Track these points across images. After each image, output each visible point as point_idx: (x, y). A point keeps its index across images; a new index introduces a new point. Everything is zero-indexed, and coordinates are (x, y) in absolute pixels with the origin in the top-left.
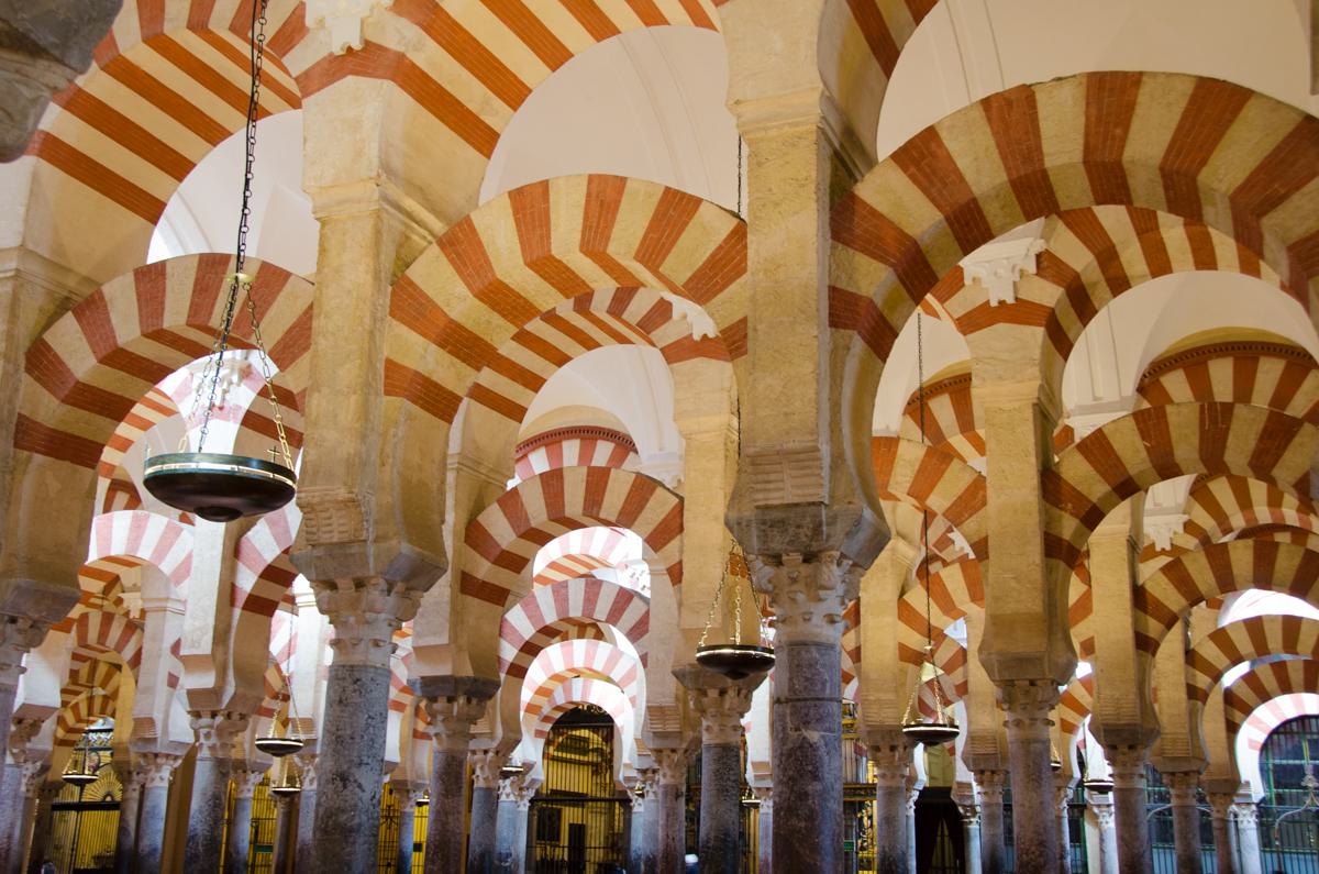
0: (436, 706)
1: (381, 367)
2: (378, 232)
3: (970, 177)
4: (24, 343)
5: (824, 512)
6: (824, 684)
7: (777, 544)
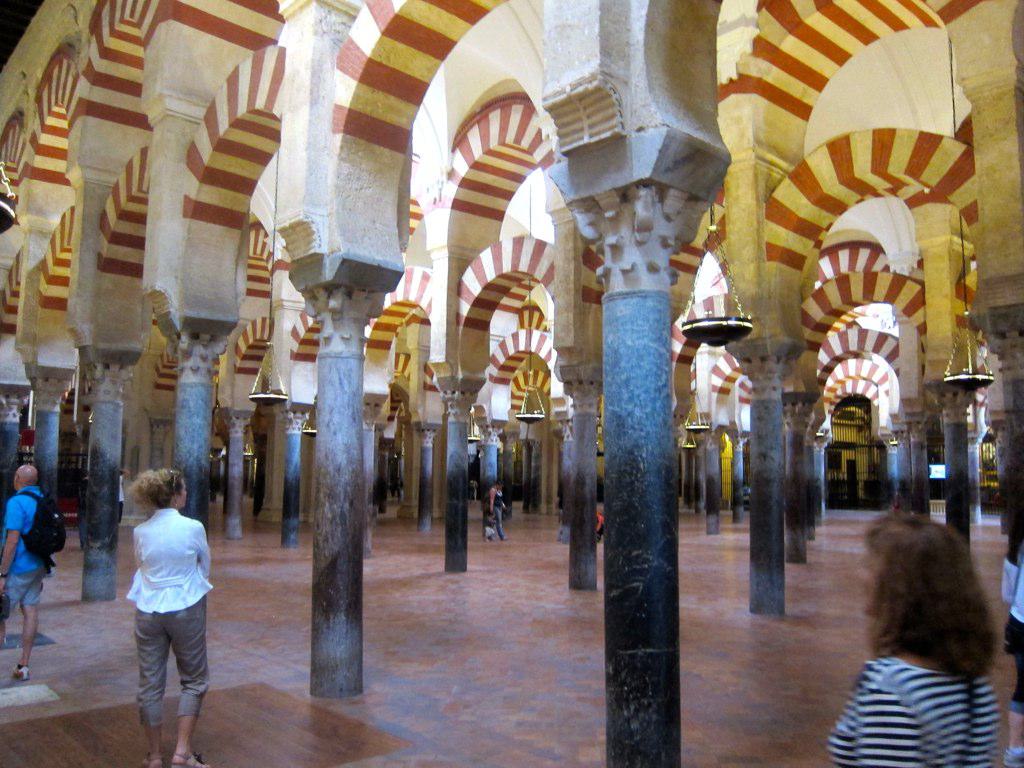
0: (786, 408)
1: (764, 247)
2: (756, 176)
4: (580, 253)
7: (1003, 327)
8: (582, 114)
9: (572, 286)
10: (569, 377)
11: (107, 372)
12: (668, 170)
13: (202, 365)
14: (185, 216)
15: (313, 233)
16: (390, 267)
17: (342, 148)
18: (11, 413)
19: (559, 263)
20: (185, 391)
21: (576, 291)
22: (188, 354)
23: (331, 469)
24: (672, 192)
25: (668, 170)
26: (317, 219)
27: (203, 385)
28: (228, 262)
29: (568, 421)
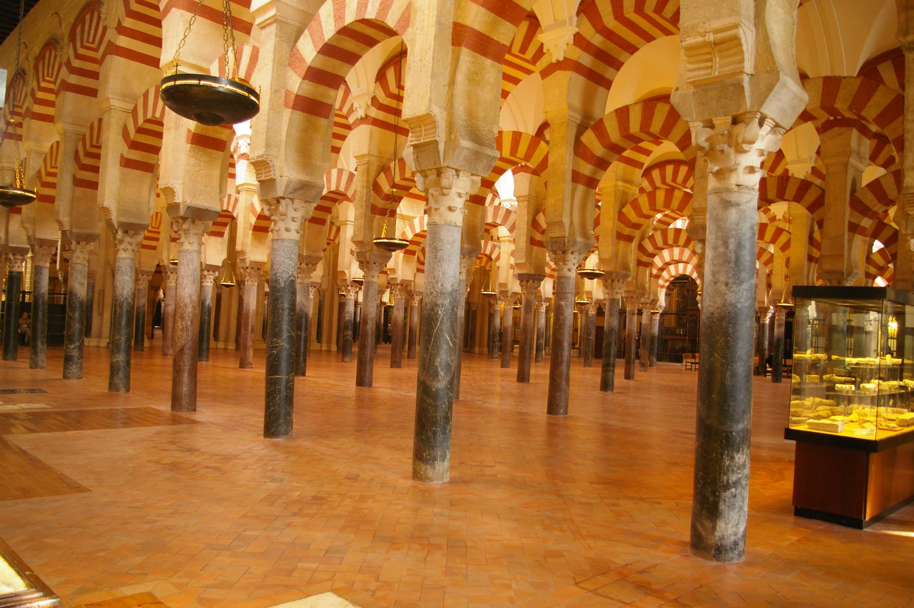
0: (523, 283)
3: (611, 136)
4: (372, 182)
5: (566, 239)
6: (566, 288)
8: (263, 168)
9: (364, 204)
10: (362, 259)
11: (78, 246)
12: (291, 193)
13: (129, 247)
14: (121, 165)
15: (175, 192)
16: (213, 209)
17: (190, 151)
18: (16, 265)
19: (359, 189)
20: (120, 261)
21: (367, 207)
22: (121, 242)
23: (182, 305)
24: (296, 200)
25: (291, 193)
26: (177, 186)
27: (130, 258)
28: (145, 191)
29: (398, 284)
